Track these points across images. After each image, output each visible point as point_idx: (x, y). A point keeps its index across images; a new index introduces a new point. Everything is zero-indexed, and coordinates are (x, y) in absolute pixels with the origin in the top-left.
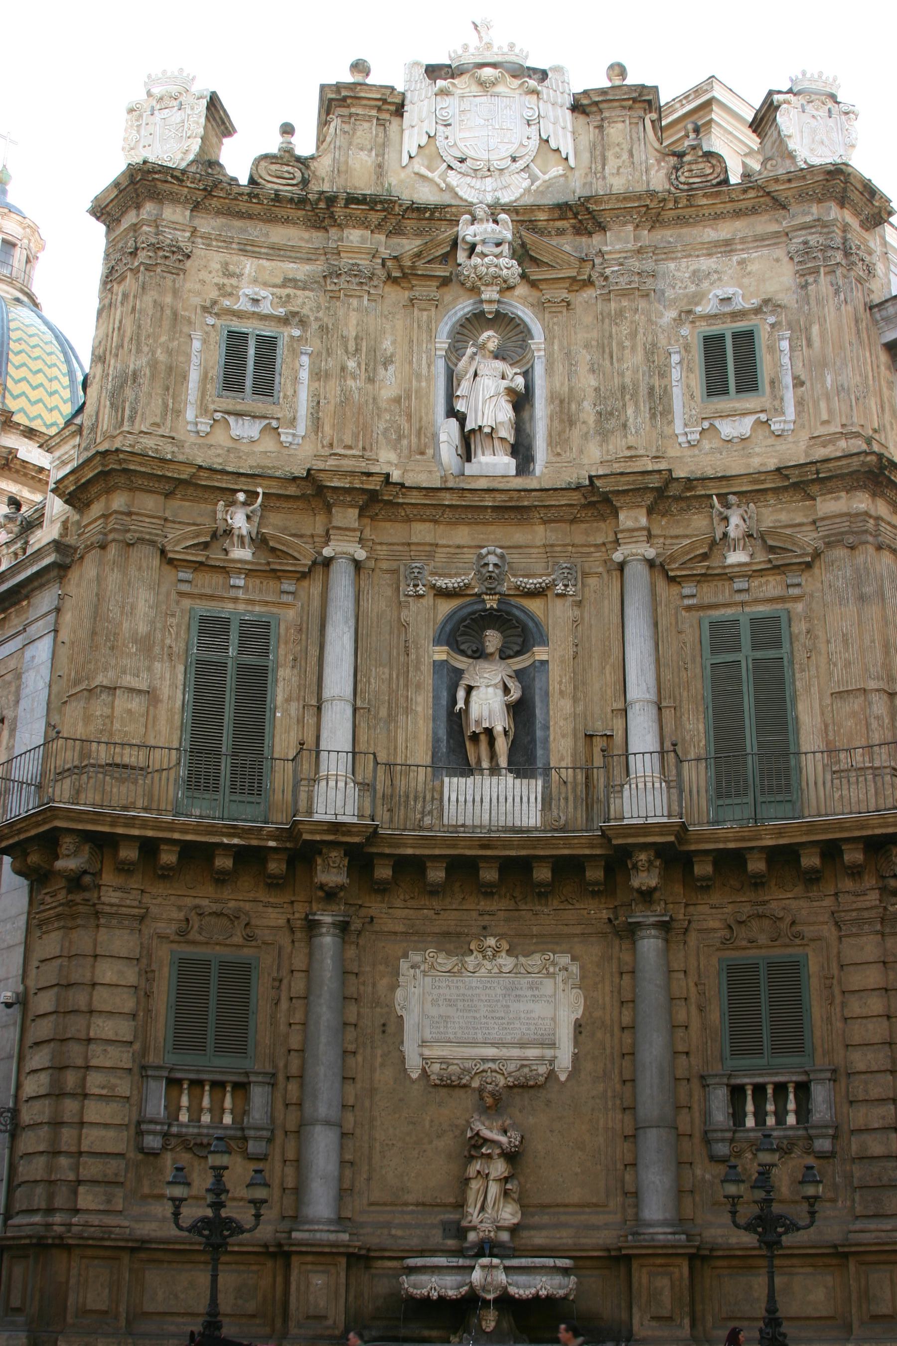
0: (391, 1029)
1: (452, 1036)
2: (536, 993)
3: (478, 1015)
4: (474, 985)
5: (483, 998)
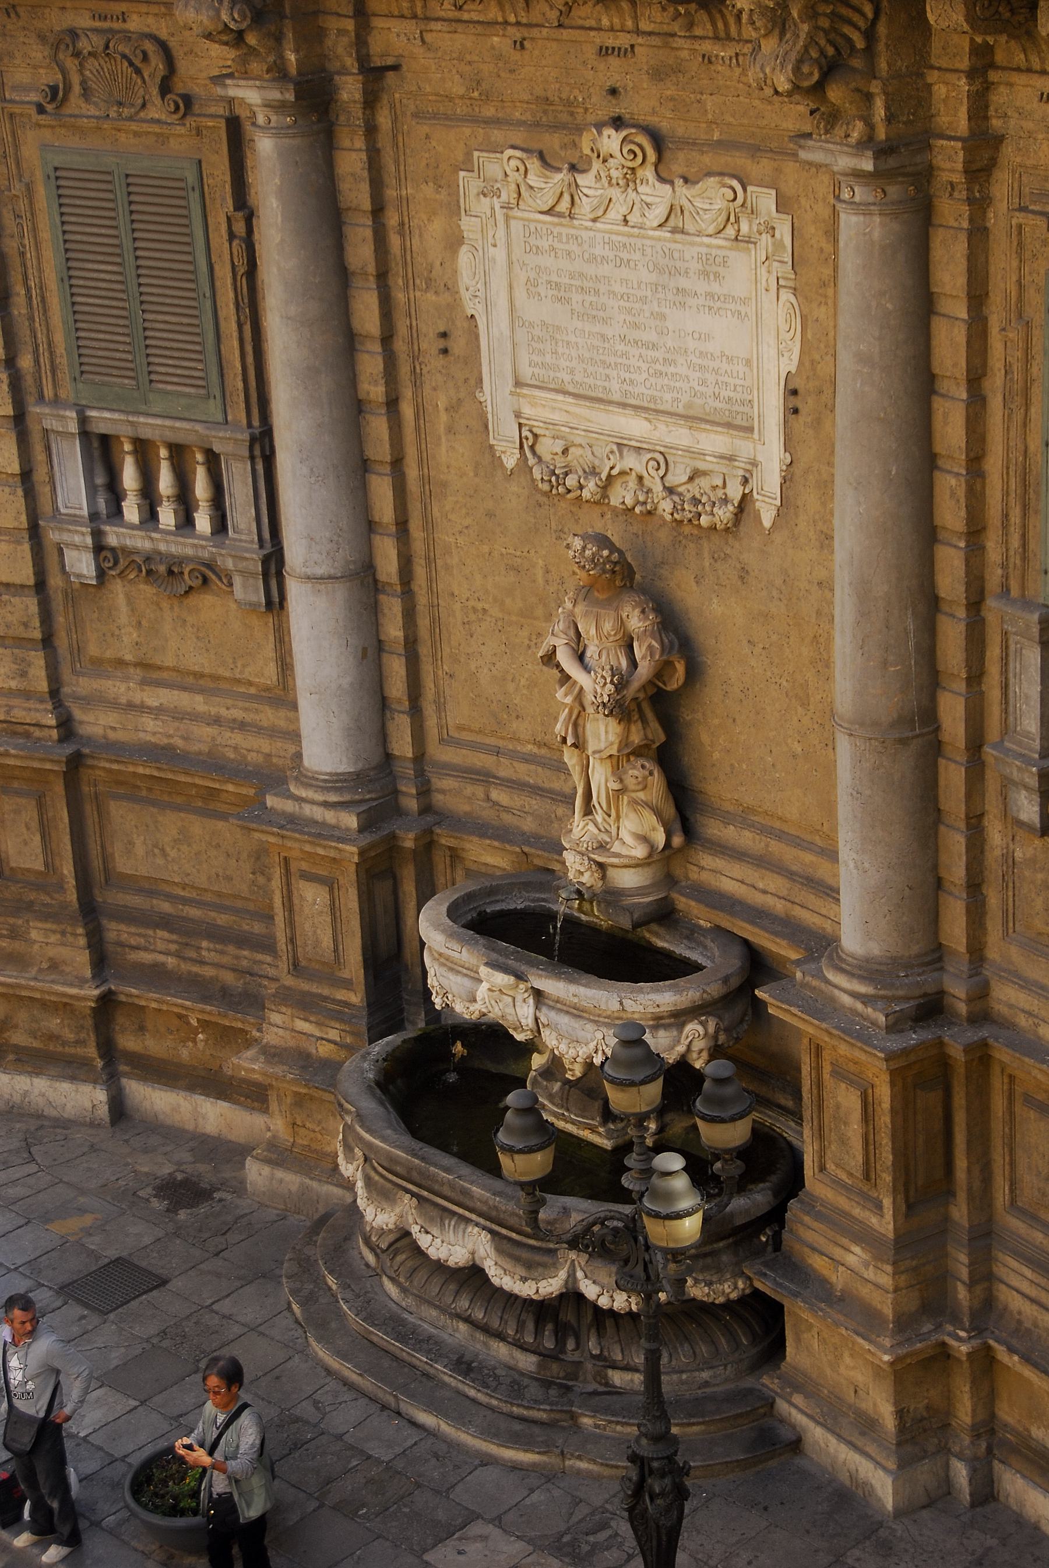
0: (458, 345)
1: (567, 378)
2: (715, 288)
3: (609, 332)
4: (598, 251)
5: (618, 288)
